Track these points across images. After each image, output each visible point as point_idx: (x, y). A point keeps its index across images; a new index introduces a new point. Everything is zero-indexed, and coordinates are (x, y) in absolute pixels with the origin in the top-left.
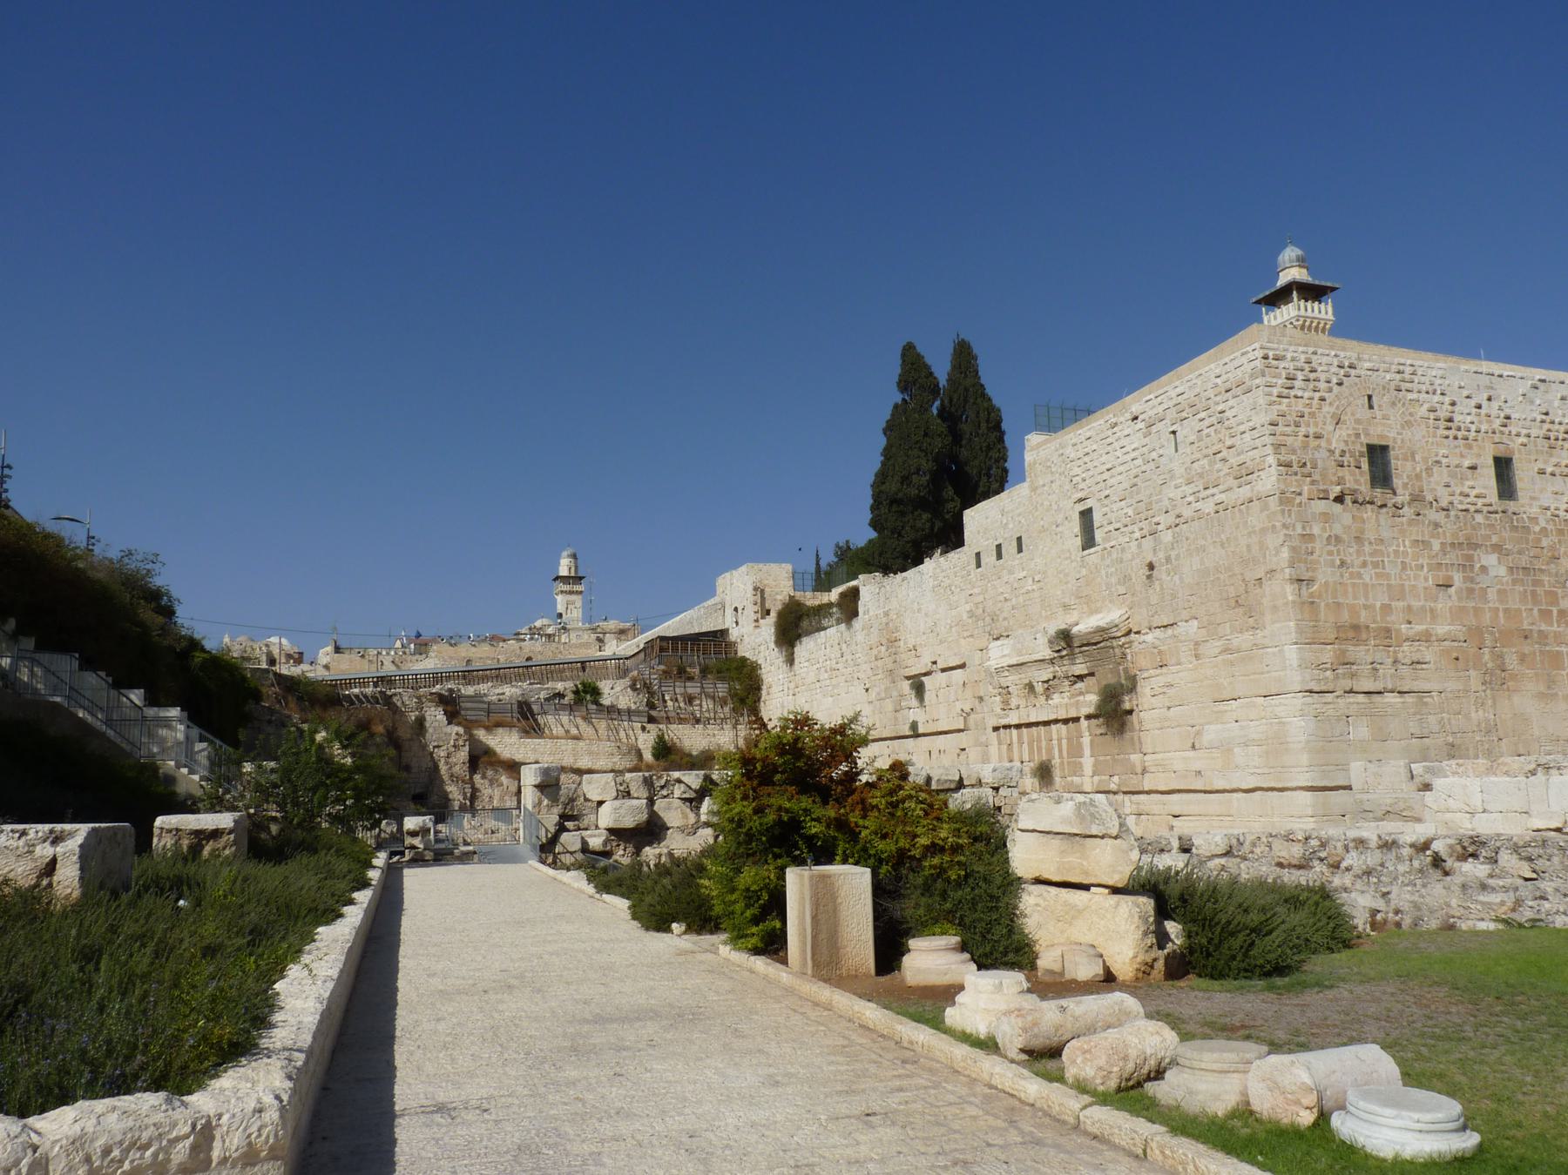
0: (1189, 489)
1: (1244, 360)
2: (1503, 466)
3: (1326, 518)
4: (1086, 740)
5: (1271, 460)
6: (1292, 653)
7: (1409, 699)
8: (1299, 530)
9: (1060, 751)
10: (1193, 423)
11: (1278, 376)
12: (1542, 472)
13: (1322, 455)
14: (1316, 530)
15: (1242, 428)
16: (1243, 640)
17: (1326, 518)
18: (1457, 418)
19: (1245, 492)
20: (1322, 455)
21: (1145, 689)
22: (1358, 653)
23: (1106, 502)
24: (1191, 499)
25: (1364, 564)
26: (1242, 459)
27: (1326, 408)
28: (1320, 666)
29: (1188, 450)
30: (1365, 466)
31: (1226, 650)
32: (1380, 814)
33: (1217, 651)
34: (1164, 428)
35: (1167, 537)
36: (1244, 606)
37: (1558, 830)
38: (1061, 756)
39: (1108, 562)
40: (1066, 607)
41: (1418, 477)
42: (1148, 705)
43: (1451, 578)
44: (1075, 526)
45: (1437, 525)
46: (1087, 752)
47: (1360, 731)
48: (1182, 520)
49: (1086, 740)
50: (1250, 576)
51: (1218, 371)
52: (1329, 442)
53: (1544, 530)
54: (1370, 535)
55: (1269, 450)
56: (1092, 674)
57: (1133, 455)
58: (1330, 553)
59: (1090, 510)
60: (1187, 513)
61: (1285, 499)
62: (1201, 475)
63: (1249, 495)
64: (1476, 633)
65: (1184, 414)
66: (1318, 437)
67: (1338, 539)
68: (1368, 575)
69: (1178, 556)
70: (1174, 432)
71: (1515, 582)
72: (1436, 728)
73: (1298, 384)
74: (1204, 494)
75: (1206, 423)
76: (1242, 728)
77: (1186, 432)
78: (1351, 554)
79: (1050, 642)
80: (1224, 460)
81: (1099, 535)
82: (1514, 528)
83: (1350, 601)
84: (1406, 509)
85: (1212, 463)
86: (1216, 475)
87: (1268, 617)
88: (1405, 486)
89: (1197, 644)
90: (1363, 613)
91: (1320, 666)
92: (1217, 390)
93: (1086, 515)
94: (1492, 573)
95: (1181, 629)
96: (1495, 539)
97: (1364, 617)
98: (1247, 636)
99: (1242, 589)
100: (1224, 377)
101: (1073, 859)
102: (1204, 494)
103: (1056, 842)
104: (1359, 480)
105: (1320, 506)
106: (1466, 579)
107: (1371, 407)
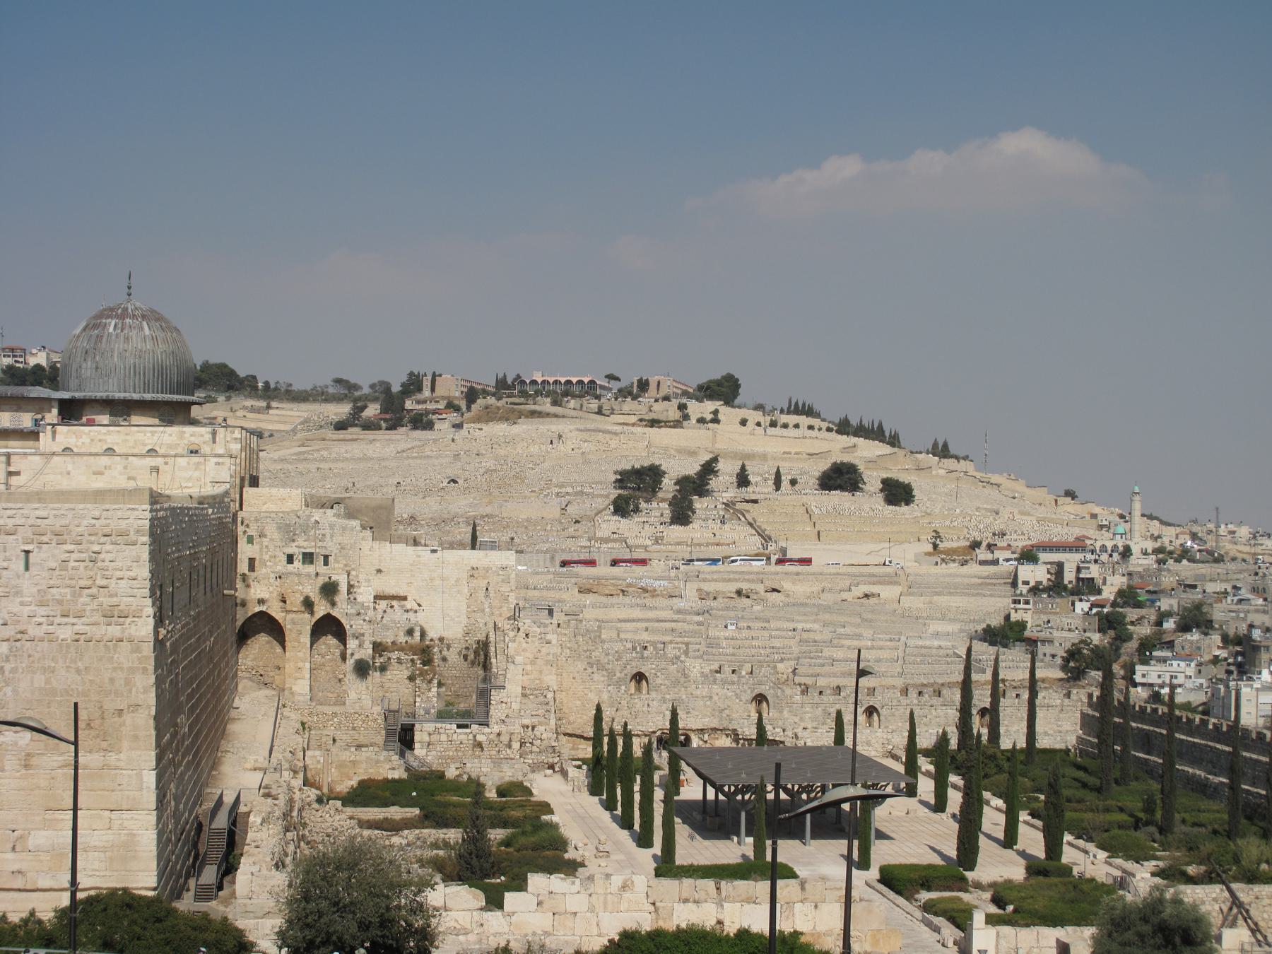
0: (42, 611)
6: (150, 778)
10: (60, 552)
15: (119, 574)
19: (114, 631)
24: (41, 620)
26: (114, 600)
29: (46, 574)
32: (261, 914)
33: (56, 764)
34: (15, 545)
48: (26, 637)
50: (110, 705)
51: (97, 513)
55: (149, 601)
60: (33, 631)
62: (60, 602)
65: (45, 539)
69: (14, 670)
70: (27, 552)
75: (74, 556)
86: (79, 607)
89: (28, 755)
99: (97, 714)
102: (58, 620)
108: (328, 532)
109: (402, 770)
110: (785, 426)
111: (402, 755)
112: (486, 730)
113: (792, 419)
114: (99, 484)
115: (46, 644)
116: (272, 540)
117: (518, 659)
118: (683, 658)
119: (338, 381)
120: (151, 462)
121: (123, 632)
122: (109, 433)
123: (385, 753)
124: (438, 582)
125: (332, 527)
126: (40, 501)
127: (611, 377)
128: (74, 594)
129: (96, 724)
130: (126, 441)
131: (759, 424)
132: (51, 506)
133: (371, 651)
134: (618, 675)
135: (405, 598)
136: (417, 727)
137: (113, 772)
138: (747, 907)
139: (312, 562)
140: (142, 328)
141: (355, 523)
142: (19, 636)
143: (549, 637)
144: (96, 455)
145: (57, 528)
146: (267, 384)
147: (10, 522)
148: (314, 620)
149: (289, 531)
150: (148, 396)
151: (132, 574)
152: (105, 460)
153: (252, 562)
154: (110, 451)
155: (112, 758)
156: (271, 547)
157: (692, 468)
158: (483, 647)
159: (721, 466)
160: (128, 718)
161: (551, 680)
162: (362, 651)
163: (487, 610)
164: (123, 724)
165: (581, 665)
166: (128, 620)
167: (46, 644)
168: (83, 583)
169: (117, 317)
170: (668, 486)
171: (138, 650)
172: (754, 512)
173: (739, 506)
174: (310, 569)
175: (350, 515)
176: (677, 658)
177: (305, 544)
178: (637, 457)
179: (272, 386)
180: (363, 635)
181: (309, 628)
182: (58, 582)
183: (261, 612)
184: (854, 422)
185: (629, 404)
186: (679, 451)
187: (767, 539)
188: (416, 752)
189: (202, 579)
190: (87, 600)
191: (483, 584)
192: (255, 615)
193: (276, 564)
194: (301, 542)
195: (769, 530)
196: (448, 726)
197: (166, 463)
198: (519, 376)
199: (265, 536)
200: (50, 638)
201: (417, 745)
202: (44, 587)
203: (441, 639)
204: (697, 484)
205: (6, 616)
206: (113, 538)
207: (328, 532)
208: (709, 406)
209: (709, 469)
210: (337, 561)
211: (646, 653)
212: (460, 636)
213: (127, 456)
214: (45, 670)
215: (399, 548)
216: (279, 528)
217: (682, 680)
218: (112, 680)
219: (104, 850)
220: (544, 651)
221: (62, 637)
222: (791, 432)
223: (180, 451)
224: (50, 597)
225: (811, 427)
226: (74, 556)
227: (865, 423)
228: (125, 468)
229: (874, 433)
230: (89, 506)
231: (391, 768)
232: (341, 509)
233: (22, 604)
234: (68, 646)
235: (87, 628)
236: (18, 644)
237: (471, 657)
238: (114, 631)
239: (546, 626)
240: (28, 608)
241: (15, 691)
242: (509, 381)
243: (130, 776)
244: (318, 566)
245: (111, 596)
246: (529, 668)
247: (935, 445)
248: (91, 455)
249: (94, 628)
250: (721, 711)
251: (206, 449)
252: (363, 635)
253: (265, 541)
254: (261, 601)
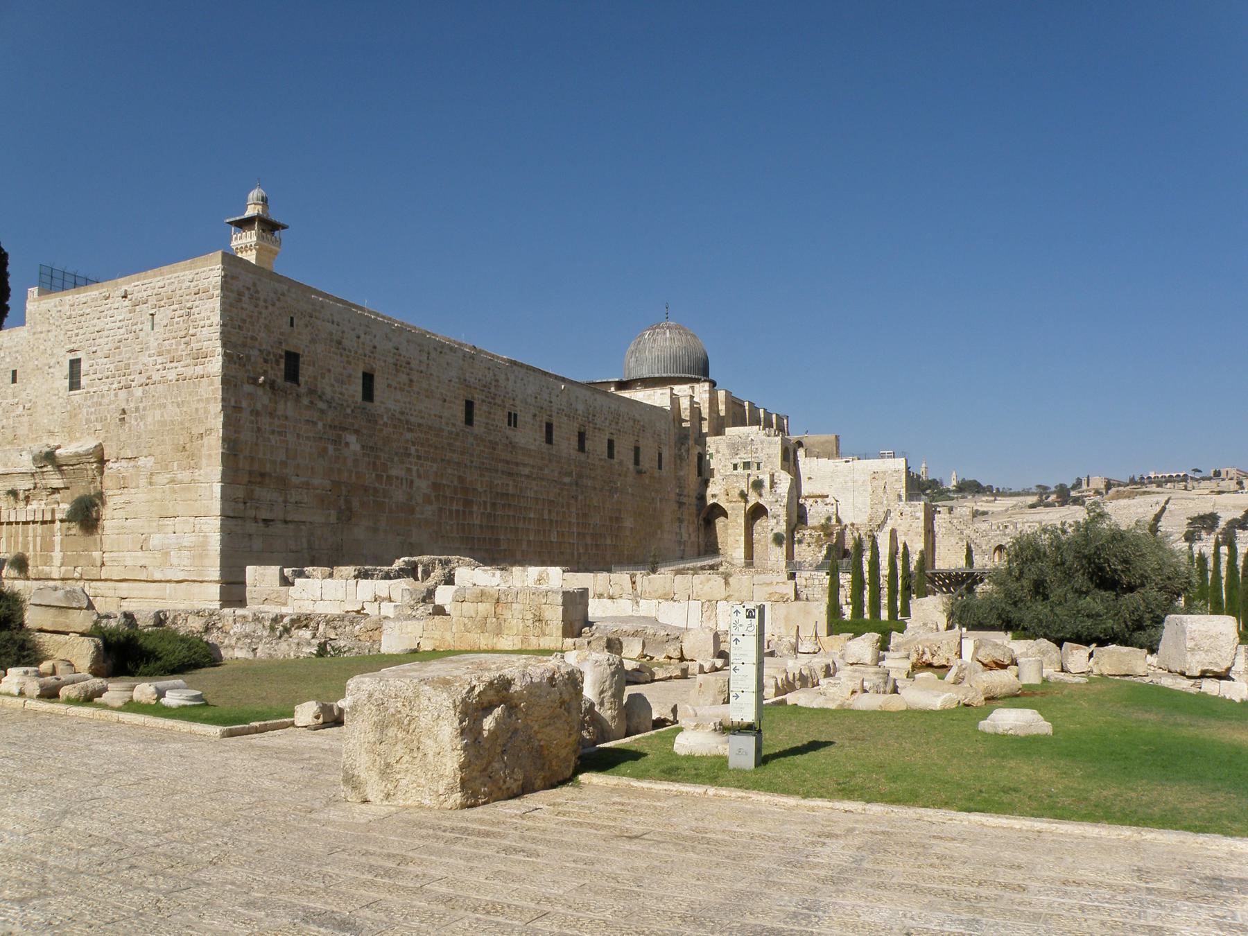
2: (368, 379)
3: (251, 396)
4: (58, 539)
5: (220, 350)
6: (217, 489)
7: (291, 526)
8: (233, 403)
9: (35, 546)
11: (232, 291)
12: (389, 386)
13: (254, 353)
14: (244, 404)
15: (202, 323)
16: (184, 476)
17: (251, 396)
18: (346, 342)
19: (199, 370)
20: (254, 353)
21: (110, 503)
22: (263, 494)
23: (92, 356)
24: (158, 367)
25: (273, 432)
26: (198, 345)
27: (262, 321)
28: (236, 500)
30: (282, 366)
31: (172, 481)
34: (146, 309)
35: (138, 392)
36: (188, 452)
37: (358, 612)
38: (35, 550)
39: (89, 403)
40: (51, 433)
41: (315, 378)
42: (110, 517)
43: (325, 450)
44: (67, 372)
45: (322, 412)
46: (58, 548)
47: (257, 544)
49: (58, 539)
52: (260, 344)
53: (385, 425)
54: (279, 413)
55: (219, 343)
56: (67, 488)
57: (118, 324)
58: (252, 422)
59: (79, 360)
61: (227, 381)
62: (169, 351)
64: (336, 484)
65: (162, 303)
66: (253, 338)
67: (258, 413)
68: (274, 439)
69: (144, 409)
71: (364, 455)
72: (305, 545)
73: (245, 299)
74: (168, 366)
76: (178, 538)
77: (162, 317)
78: (265, 421)
79: (34, 459)
80: (187, 344)
81: (84, 381)
82: (369, 421)
83: (261, 456)
84: (305, 401)
85: (178, 344)
87: (204, 461)
88: (306, 382)
90: (268, 466)
91: (236, 500)
93: (75, 364)
94: (352, 447)
95: (142, 461)
96: (356, 427)
97: (268, 468)
98: (188, 473)
100: (194, 283)
101: (61, 619)
102: (169, 365)
103: (52, 611)
104: (278, 373)
105: (248, 388)
106: (335, 450)
107: (292, 325)
124: (850, 484)
125: (762, 443)
129: (188, 446)
138: (664, 604)
147: (145, 294)
151: (209, 322)
160: (205, 439)
164: (202, 446)
167: (160, 387)
171: (212, 384)
190: (183, 346)
194: (742, 454)
200: (164, 380)
203: (853, 525)
207: (759, 446)
218: (197, 409)
219: (189, 549)
226: (177, 313)
238: (199, 370)
244: (754, 471)
253: (719, 455)
254: (714, 496)
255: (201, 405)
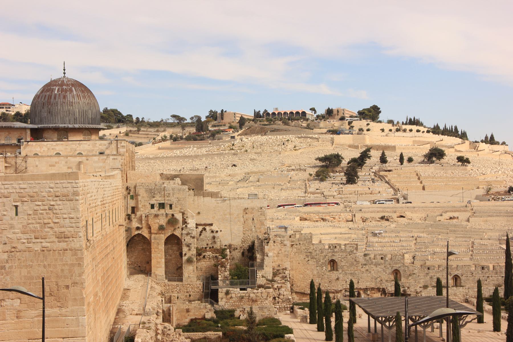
1: (69, 185)
15: (65, 216)
19: (63, 245)
26: (63, 230)
29: (26, 217)
34: (9, 203)
51: (52, 185)
60: (20, 247)
62: (34, 232)
63: (65, 247)
65: (25, 199)
70: (16, 207)
74: (34, 240)
75: (42, 207)
80: (52, 228)
86: (44, 234)
92: (50, 194)
98: (57, 310)
102: (34, 240)
108: (171, 192)
109: (213, 313)
110: (405, 131)
111: (212, 304)
112: (255, 291)
113: (408, 127)
114: (53, 171)
115: (27, 253)
116: (143, 197)
117: (270, 254)
118: (355, 252)
119: (174, 116)
120: (78, 159)
121: (68, 245)
122: (57, 145)
123: (204, 304)
124: (228, 216)
126: (22, 180)
127: (313, 109)
128: (41, 227)
130: (66, 149)
131: (391, 130)
132: (29, 182)
133: (195, 252)
134: (322, 261)
135: (211, 225)
136: (220, 290)
137: (64, 318)
139: (163, 208)
140: (71, 91)
141: (186, 187)
142: (13, 250)
143: (285, 242)
144: (51, 156)
145: (32, 194)
146: (138, 118)
148: (166, 237)
149: (152, 193)
150: (77, 126)
152: (56, 159)
153: (133, 208)
154: (58, 154)
155: (64, 310)
156: (143, 200)
157: (356, 154)
158: (251, 249)
159: (372, 153)
160: (71, 289)
161: (287, 265)
162: (191, 252)
163: (254, 230)
165: (302, 257)
166: (71, 239)
168: (46, 221)
169: (59, 85)
170: (344, 163)
172: (390, 176)
173: (382, 173)
174: (162, 211)
175: (183, 184)
176: (352, 252)
177: (160, 199)
178: (329, 150)
179: (141, 120)
180: (191, 244)
181: (163, 241)
182: (34, 222)
183: (139, 234)
184: (442, 128)
185: (322, 124)
186: (350, 146)
187: (396, 190)
188: (220, 303)
189: (108, 218)
191: (250, 216)
192: (135, 236)
193: (145, 210)
195: (397, 185)
196: (235, 290)
197: (87, 160)
198: (266, 111)
199: (139, 195)
200: (29, 250)
201: (219, 300)
202: (25, 224)
204: (360, 162)
205: (6, 240)
206: (61, 198)
207: (171, 192)
208: (363, 123)
209: (365, 155)
210: (176, 207)
211: (336, 250)
212: (240, 243)
213: (67, 157)
214: (26, 267)
215: (208, 199)
216: (146, 191)
217: (355, 263)
218: (62, 270)
220: (283, 250)
221: (36, 249)
222: (408, 134)
223: (94, 153)
224: (28, 229)
225: (418, 131)
227: (448, 127)
228: (66, 162)
229: (452, 132)
230: (48, 182)
231: (207, 311)
232: (178, 180)
233: (14, 233)
234: (39, 254)
235: (48, 245)
236: (13, 254)
237: (246, 253)
238: (63, 245)
239: (283, 237)
240: (18, 235)
241: (11, 278)
242: (261, 113)
243: (73, 320)
245: (61, 227)
246: (276, 258)
247: (486, 138)
248: (48, 156)
249: (52, 244)
250: (376, 279)
251: (107, 152)
252: (191, 244)
254: (138, 228)
255: (67, 267)
